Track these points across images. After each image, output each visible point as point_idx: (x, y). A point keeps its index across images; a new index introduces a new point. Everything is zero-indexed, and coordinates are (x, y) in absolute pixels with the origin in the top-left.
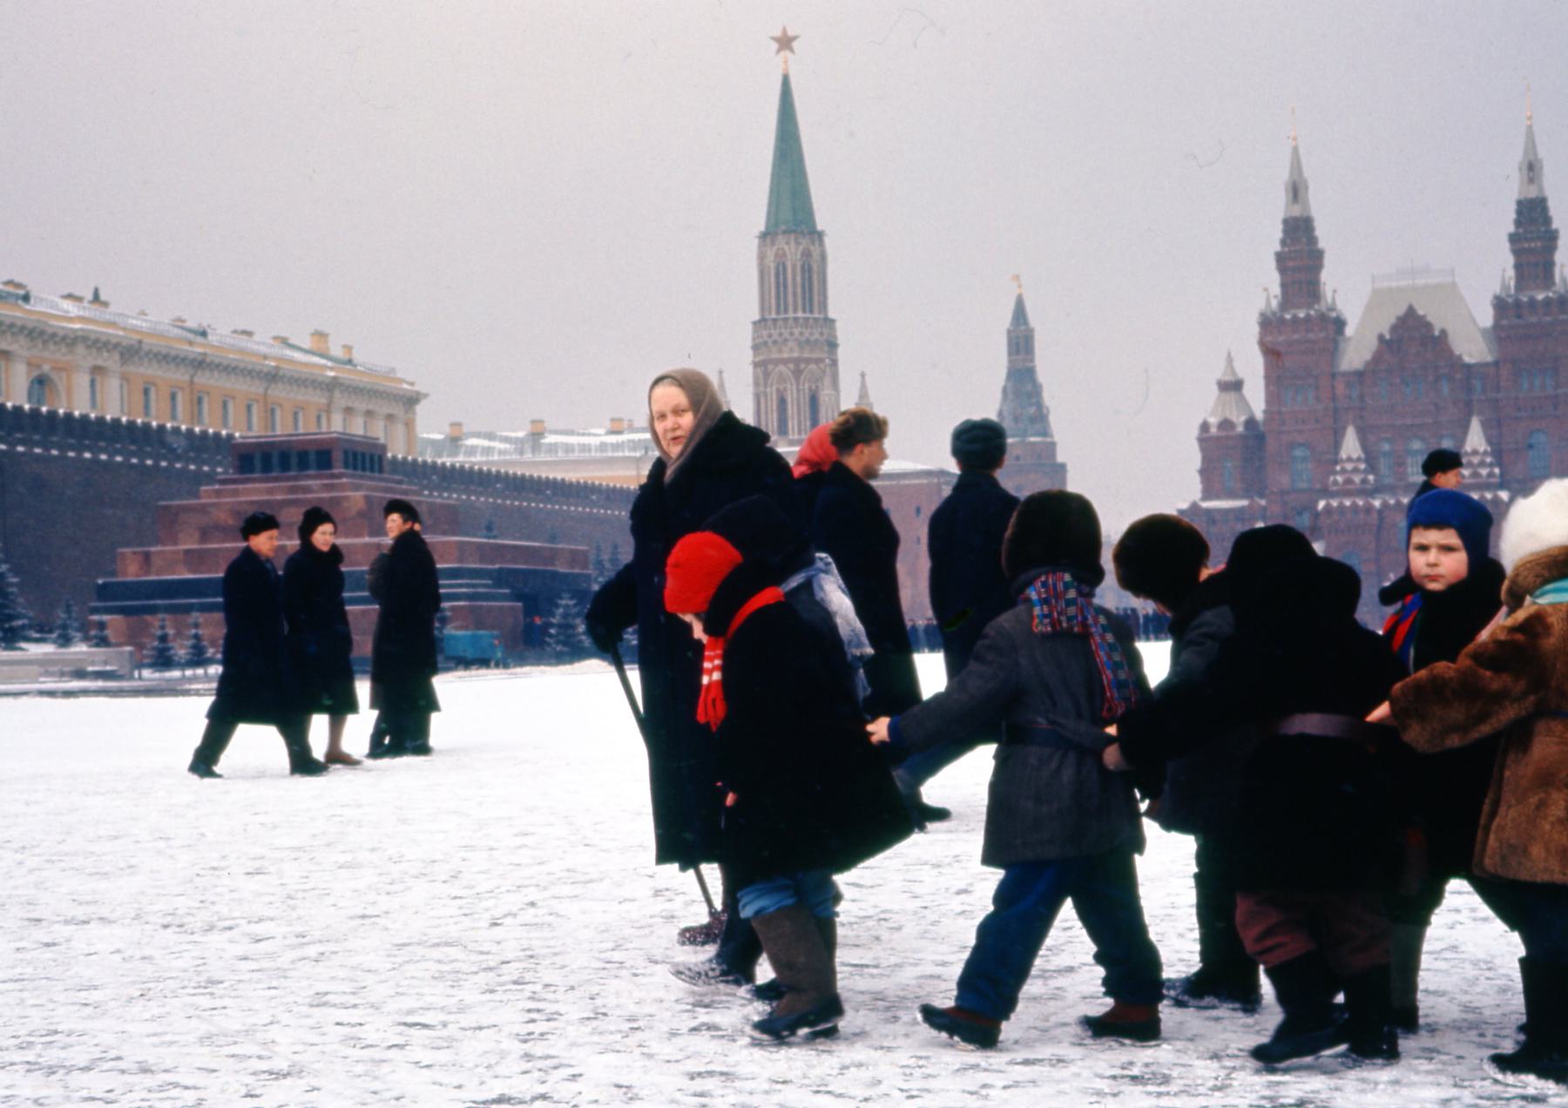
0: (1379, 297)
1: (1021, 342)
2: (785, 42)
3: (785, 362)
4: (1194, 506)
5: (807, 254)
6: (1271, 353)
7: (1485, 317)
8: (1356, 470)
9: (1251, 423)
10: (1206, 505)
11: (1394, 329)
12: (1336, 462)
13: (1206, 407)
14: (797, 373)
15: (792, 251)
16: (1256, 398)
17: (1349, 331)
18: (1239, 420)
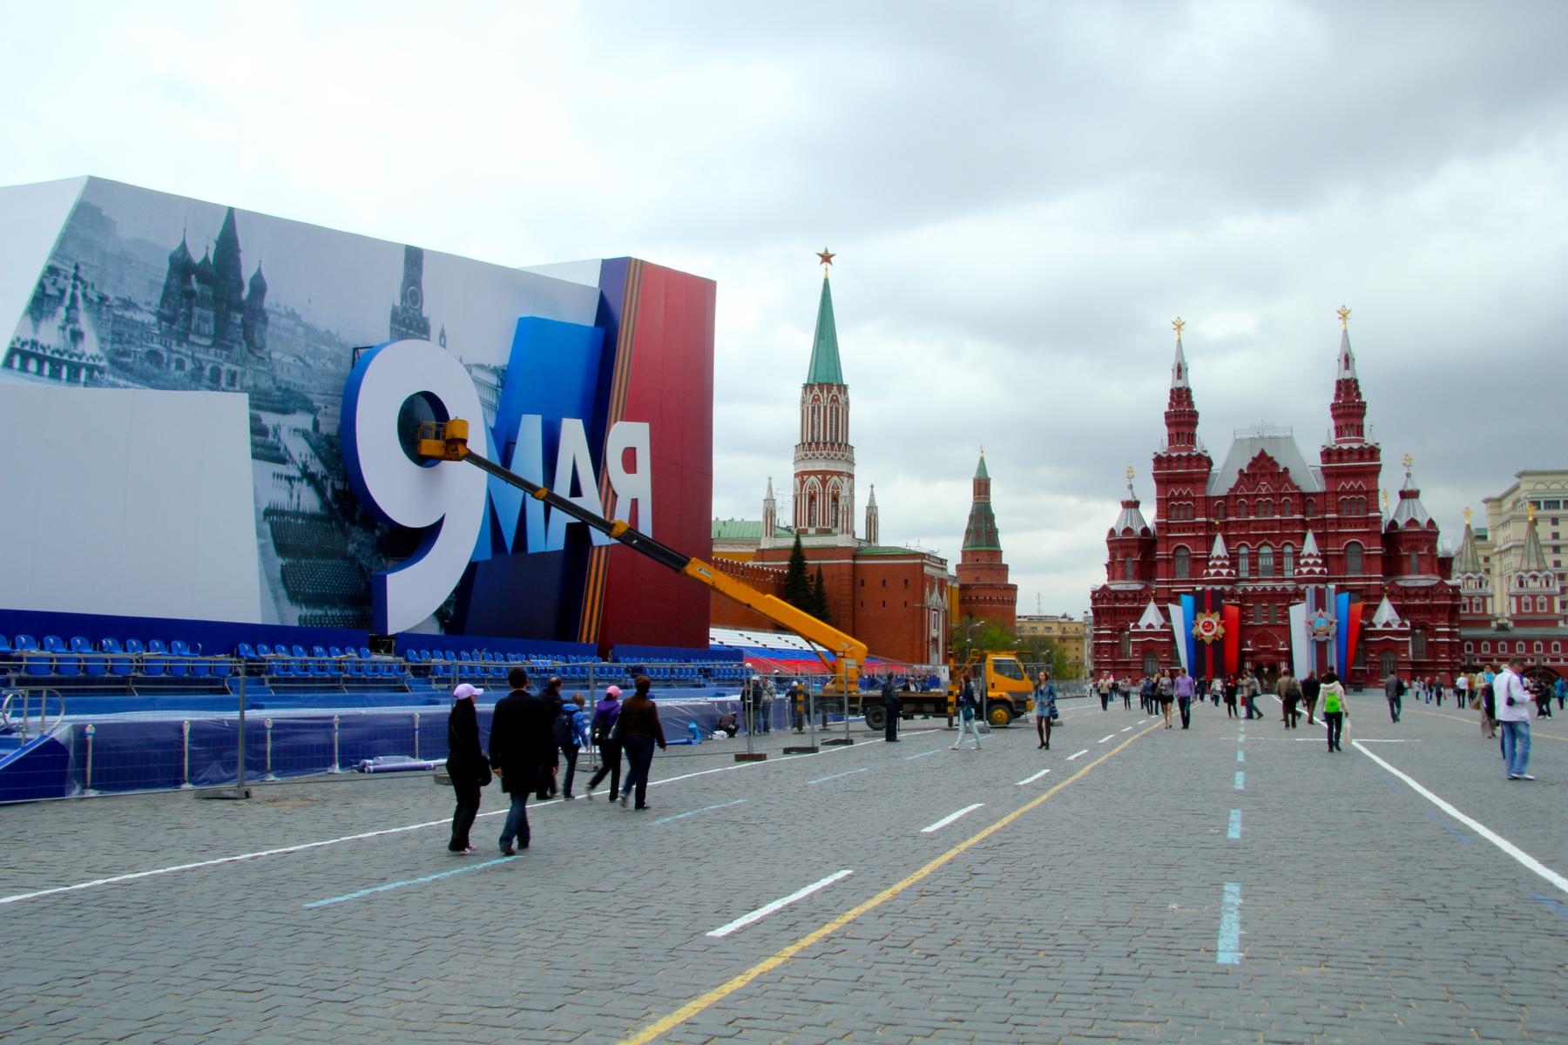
0: (1238, 443)
1: (982, 487)
2: (826, 258)
3: (815, 473)
4: (1105, 588)
5: (835, 400)
6: (1162, 482)
7: (1317, 462)
8: (1223, 566)
9: (1145, 531)
10: (1113, 588)
11: (1251, 466)
12: (1208, 560)
13: (1111, 516)
14: (824, 482)
15: (825, 397)
16: (1149, 515)
17: (1217, 467)
18: (1138, 530)
